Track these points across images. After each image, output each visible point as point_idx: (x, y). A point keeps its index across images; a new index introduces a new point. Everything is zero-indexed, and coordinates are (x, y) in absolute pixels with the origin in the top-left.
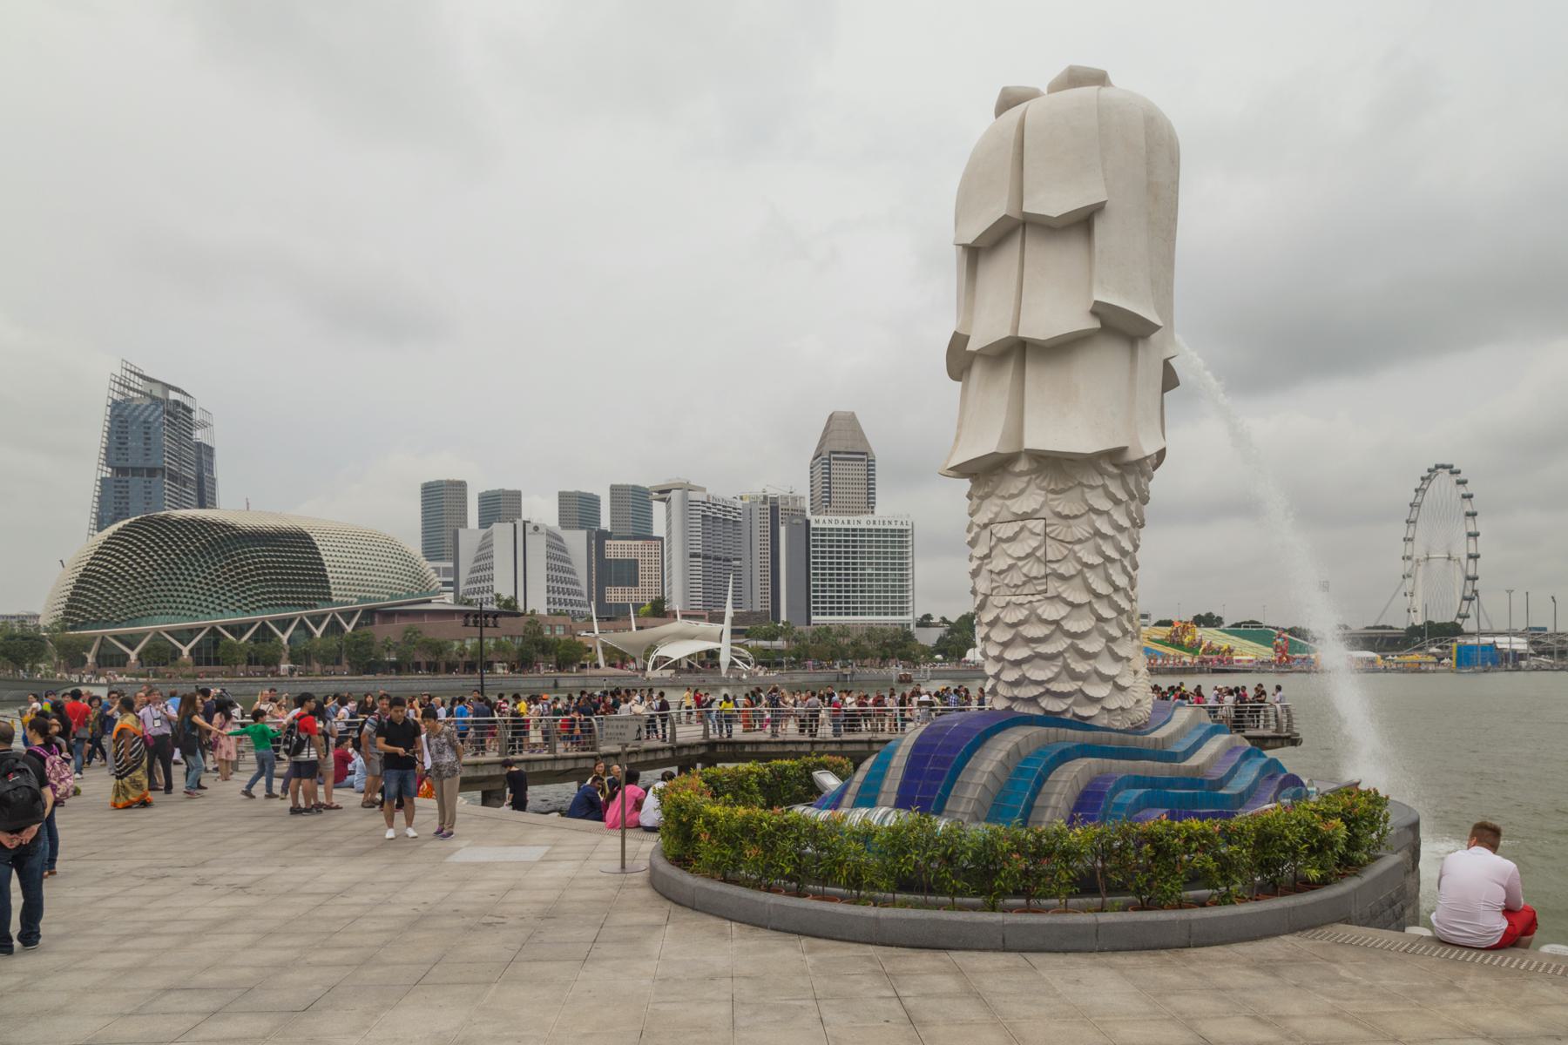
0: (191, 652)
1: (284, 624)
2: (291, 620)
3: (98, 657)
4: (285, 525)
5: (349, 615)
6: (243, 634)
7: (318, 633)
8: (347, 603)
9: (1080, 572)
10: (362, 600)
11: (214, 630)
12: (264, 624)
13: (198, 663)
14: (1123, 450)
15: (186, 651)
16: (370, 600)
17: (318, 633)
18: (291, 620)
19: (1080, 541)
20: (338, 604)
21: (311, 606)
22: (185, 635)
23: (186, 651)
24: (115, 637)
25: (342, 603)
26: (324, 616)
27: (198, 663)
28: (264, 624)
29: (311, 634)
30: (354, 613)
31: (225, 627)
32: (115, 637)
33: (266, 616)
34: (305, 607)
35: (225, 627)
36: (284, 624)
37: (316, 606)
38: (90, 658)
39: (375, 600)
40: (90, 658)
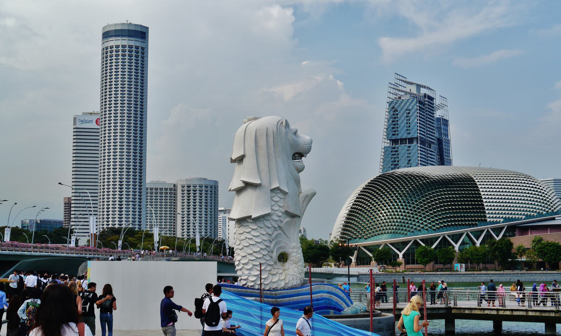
0: (404, 255)
1: (455, 238)
2: (461, 235)
3: (357, 259)
4: (459, 173)
5: (498, 230)
6: (432, 244)
7: (478, 243)
8: (496, 222)
9: (243, 248)
10: (506, 220)
11: (416, 243)
12: (444, 237)
13: (407, 263)
14: (251, 216)
15: (401, 255)
16: (512, 220)
17: (478, 243)
18: (461, 235)
19: (242, 240)
20: (490, 223)
21: (473, 225)
22: (400, 245)
23: (401, 255)
24: (365, 247)
25: (493, 223)
26: (482, 231)
27: (407, 263)
28: (444, 237)
29: (474, 243)
30: (502, 228)
31: (422, 240)
32: (365, 247)
33: (445, 233)
34: (470, 226)
35: (422, 240)
36: (455, 238)
37: (476, 225)
38: (353, 259)
39: (515, 219)
40: (353, 259)
